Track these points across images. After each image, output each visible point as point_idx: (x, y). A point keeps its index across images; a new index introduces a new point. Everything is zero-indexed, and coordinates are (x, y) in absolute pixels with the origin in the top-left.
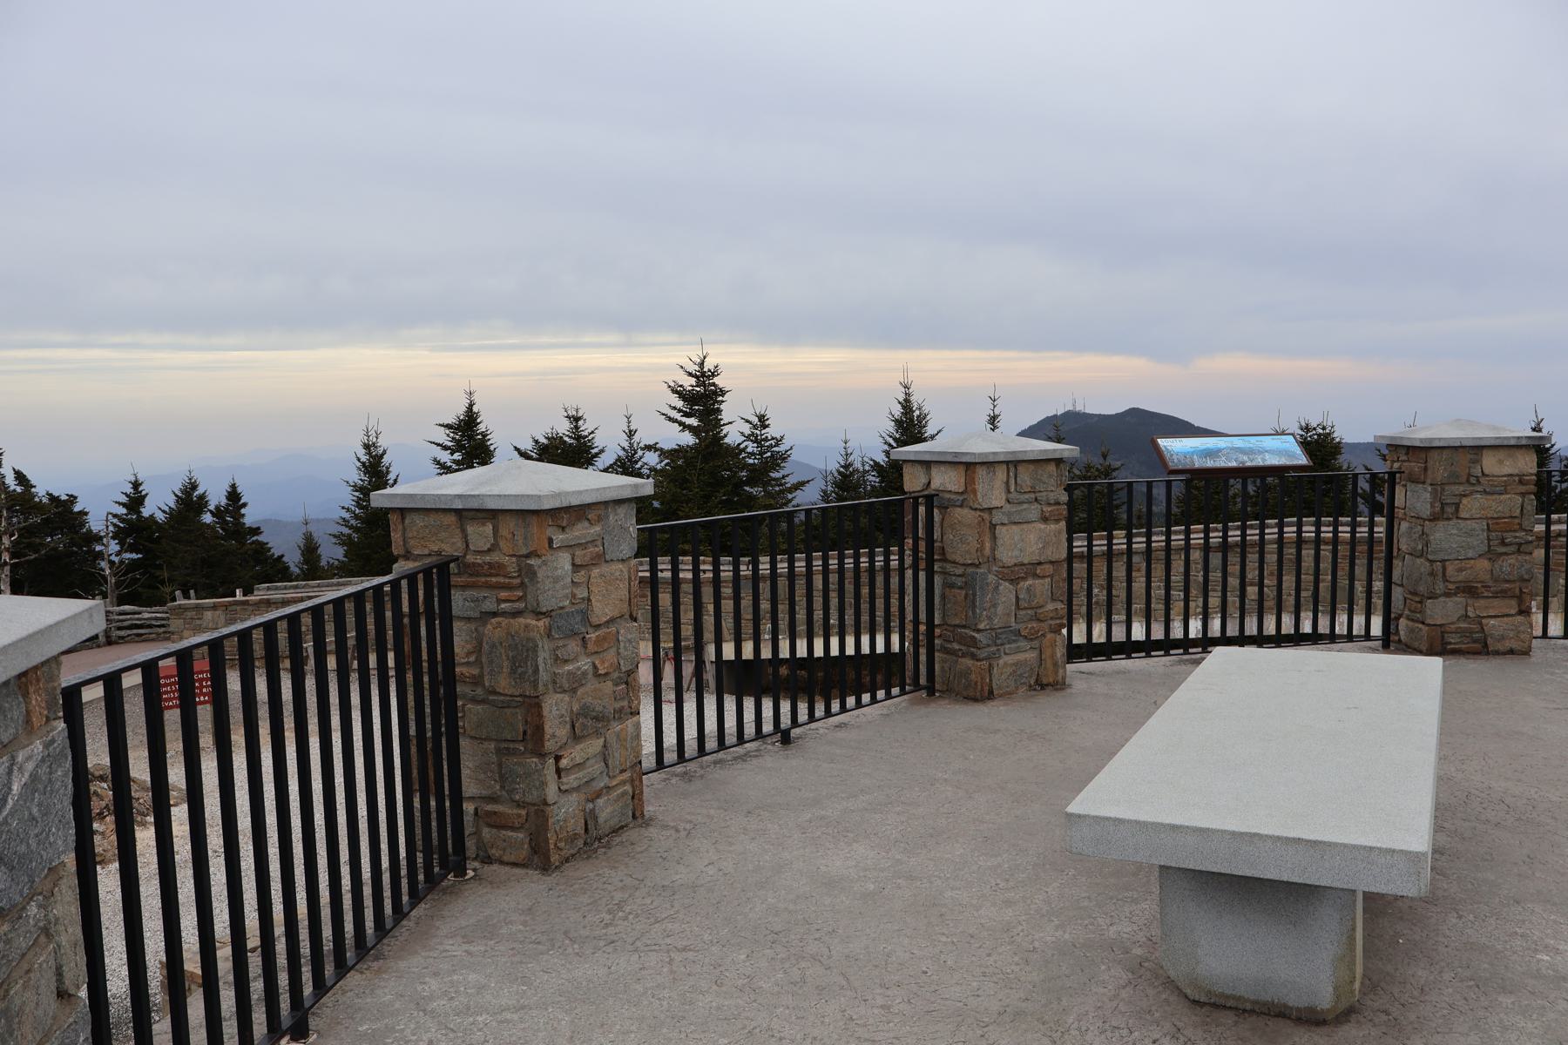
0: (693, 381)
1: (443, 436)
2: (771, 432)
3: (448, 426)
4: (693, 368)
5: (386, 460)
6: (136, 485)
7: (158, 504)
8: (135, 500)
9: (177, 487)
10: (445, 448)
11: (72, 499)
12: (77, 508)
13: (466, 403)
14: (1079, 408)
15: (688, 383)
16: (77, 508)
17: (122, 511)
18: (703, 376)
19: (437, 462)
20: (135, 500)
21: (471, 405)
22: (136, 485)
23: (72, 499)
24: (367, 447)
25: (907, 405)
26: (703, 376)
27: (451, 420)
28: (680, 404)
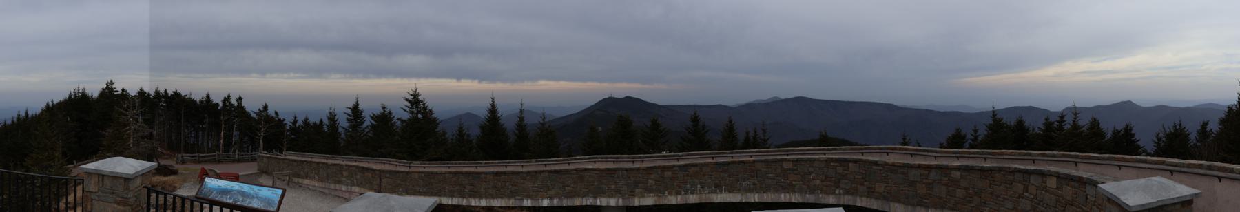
0: (412, 97)
1: (349, 111)
2: (434, 116)
3: (350, 108)
4: (411, 93)
5: (337, 117)
6: (295, 118)
7: (300, 122)
8: (295, 122)
9: (303, 119)
10: (349, 115)
11: (284, 120)
12: (285, 122)
13: (355, 101)
14: (613, 96)
15: (411, 98)
16: (285, 122)
17: (291, 124)
18: (415, 95)
19: (347, 119)
20: (295, 122)
21: (357, 102)
22: (295, 118)
23: (284, 120)
24: (330, 113)
25: (493, 105)
26: (415, 95)
27: (351, 106)
28: (409, 104)
